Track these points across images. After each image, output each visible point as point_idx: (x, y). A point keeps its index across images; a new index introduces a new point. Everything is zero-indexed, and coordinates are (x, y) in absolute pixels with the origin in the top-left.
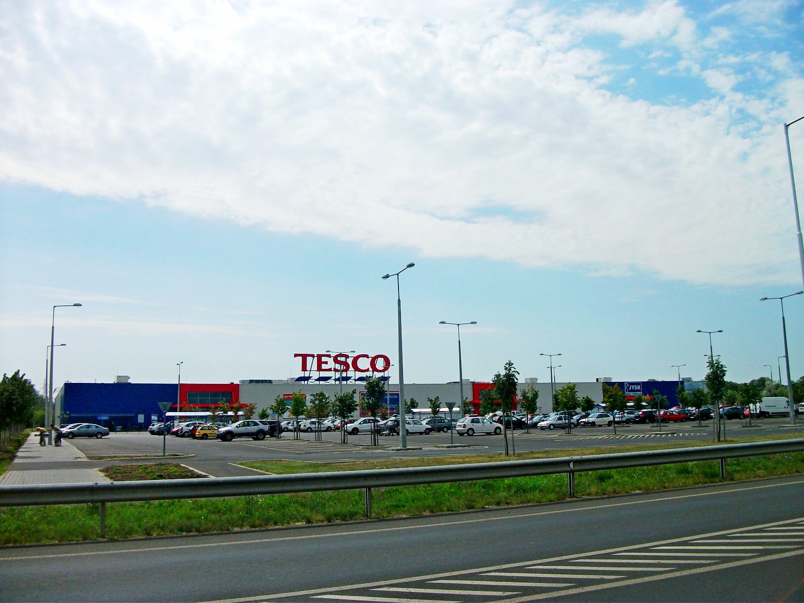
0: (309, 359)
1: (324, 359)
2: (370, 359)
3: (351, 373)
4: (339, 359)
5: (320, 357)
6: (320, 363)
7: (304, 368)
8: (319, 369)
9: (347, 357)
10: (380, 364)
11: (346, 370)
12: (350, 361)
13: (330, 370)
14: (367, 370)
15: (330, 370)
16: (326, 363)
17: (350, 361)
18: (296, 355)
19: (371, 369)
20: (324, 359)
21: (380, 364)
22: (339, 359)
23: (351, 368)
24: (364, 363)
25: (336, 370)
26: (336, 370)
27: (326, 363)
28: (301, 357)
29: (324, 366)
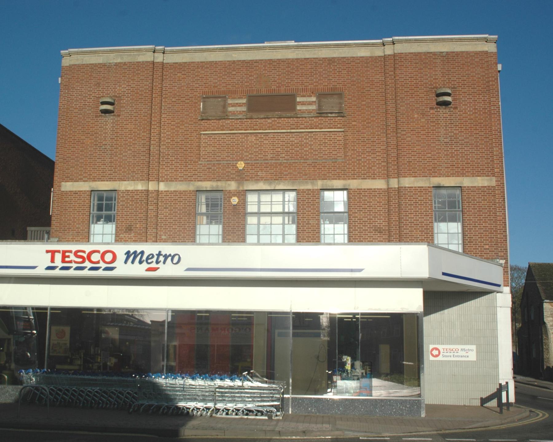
0: (56, 254)
1: (67, 254)
2: (101, 252)
3: (88, 264)
4: (79, 254)
5: (64, 252)
6: (64, 257)
7: (53, 261)
8: (63, 261)
9: (84, 252)
10: (109, 257)
11: (83, 262)
12: (85, 255)
13: (70, 262)
14: (98, 262)
15: (70, 262)
16: (68, 257)
17: (85, 255)
18: (48, 252)
19: (101, 261)
20: (67, 254)
21: (109, 257)
22: (79, 254)
23: (87, 261)
24: (96, 257)
25: (76, 262)
26: (76, 262)
27: (68, 257)
28: (50, 254)
29: (67, 259)
